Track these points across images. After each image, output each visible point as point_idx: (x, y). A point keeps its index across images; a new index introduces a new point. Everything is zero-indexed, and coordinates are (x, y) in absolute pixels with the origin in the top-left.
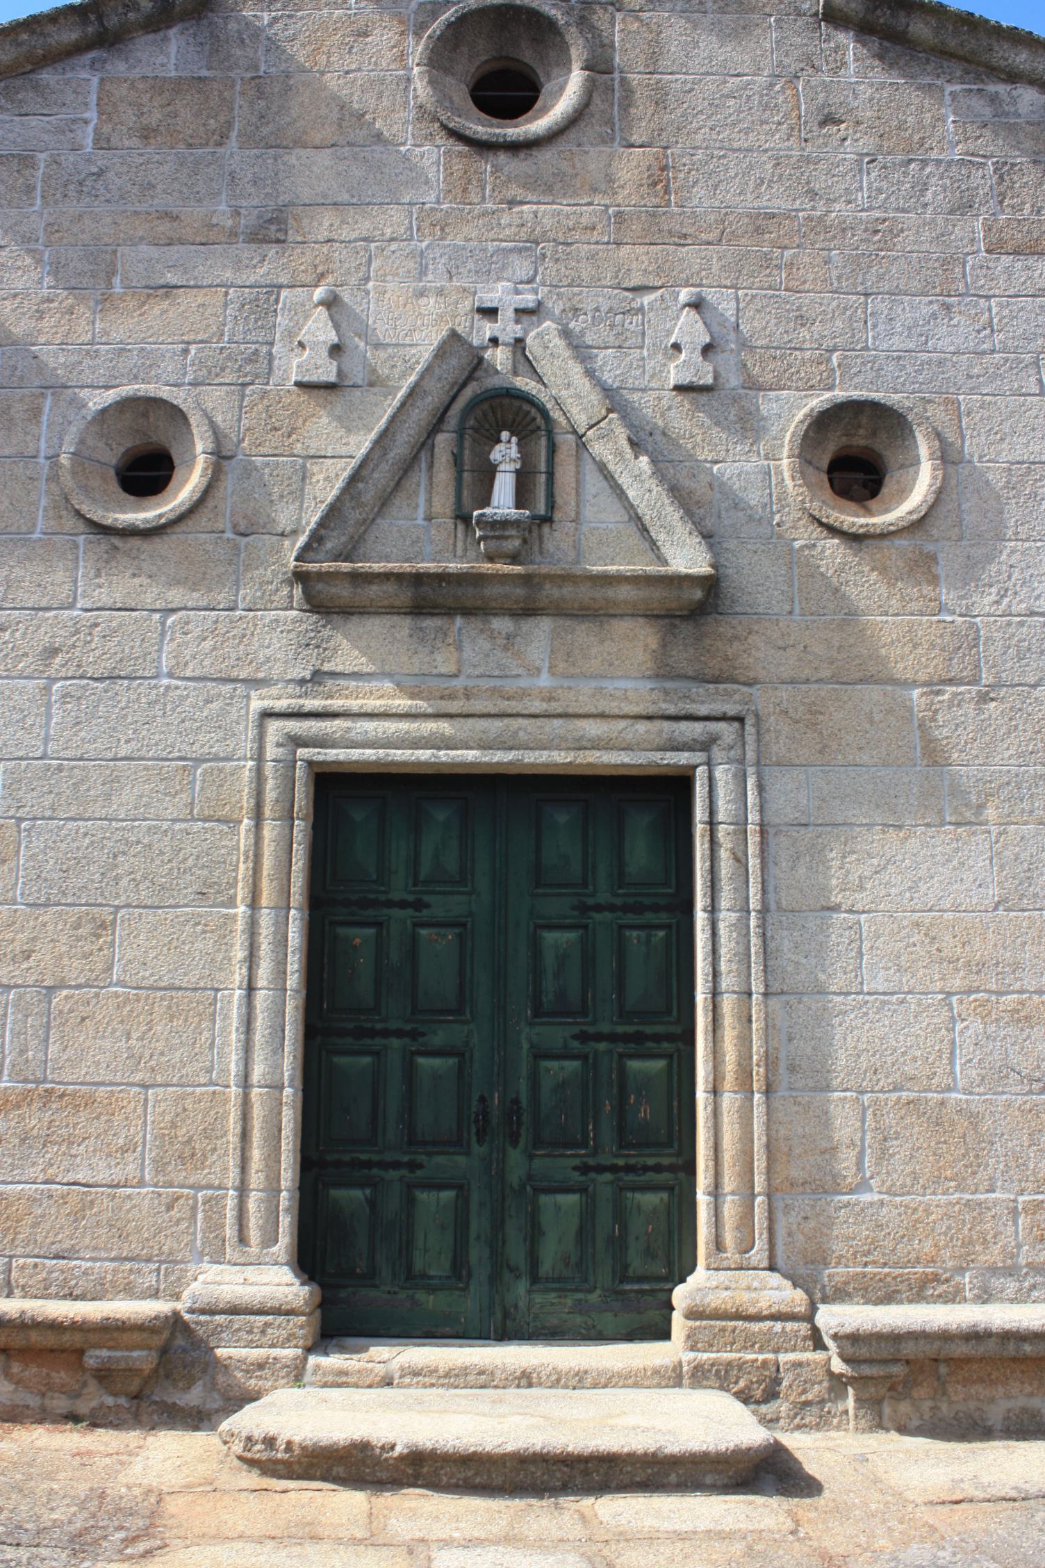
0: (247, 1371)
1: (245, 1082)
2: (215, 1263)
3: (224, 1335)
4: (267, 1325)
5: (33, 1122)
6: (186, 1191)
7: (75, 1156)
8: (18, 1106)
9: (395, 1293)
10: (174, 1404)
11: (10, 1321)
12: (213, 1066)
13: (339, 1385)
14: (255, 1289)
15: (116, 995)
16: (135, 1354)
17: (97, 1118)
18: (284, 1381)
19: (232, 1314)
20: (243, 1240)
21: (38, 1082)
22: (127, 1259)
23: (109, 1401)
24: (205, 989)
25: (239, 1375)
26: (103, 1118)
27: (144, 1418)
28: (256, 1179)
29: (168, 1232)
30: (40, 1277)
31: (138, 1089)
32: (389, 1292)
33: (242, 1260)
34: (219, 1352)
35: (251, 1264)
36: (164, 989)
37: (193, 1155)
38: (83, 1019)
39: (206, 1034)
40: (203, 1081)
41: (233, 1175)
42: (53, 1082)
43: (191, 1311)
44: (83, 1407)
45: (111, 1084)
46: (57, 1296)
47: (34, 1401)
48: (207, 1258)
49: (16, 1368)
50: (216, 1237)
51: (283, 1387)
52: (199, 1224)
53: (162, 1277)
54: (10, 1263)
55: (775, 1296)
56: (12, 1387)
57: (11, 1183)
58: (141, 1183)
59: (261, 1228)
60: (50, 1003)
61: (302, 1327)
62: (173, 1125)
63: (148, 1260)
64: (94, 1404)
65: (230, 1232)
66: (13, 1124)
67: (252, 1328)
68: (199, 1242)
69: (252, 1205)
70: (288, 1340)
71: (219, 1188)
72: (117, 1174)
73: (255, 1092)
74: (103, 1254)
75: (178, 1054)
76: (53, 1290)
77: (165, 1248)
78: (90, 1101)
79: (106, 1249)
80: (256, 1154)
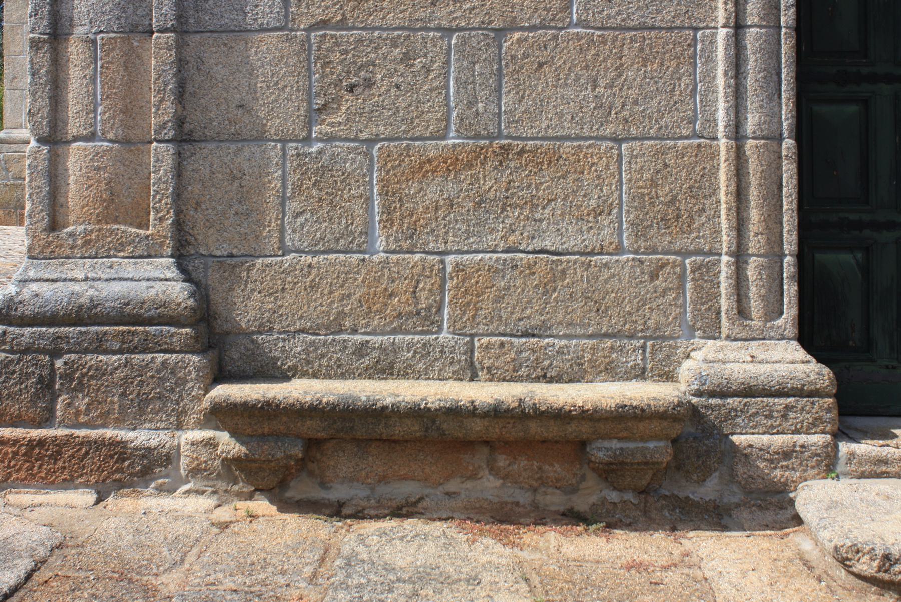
0: (771, 461)
1: (737, 133)
2: (709, 338)
3: (739, 420)
4: (788, 408)
5: (489, 184)
6: (672, 258)
7: (541, 221)
8: (469, 165)
9: (894, 368)
10: (687, 498)
11: (508, 410)
12: (695, 116)
13: (879, 476)
14: (768, 368)
15: (578, 37)
16: (651, 445)
17: (564, 177)
18: (816, 471)
19: (746, 396)
20: (742, 312)
21: (491, 137)
22: (606, 335)
23: (614, 496)
24: (682, 28)
25: (762, 465)
26: (571, 177)
27: (654, 514)
28: (755, 243)
29: (654, 305)
30: (508, 357)
31: (610, 144)
32: (887, 367)
33: (743, 335)
34: (735, 438)
35: (754, 339)
36: (634, 28)
37: (678, 217)
38: (540, 65)
39: (685, 80)
40: (685, 132)
41: (726, 239)
42: (507, 137)
43: (699, 393)
44: (582, 504)
45: (578, 138)
46: (529, 379)
47: (524, 498)
48: (698, 333)
49: (502, 461)
50: (709, 309)
51: (814, 478)
52: (688, 295)
53: (647, 355)
54: (472, 342)
55: (783, 369)
56: (499, 483)
57: (467, 252)
58: (619, 250)
59: (763, 298)
60: (500, 47)
61: (829, 410)
62: (653, 183)
63: (631, 336)
64: (593, 499)
65: (725, 303)
66: (464, 186)
67: (771, 411)
68: (689, 316)
69: (751, 273)
70: (814, 425)
71: (710, 253)
72: (590, 240)
73: (750, 143)
74: (579, 331)
75: (654, 103)
76: (523, 371)
77: (650, 323)
78: (554, 158)
79: (582, 325)
80: (754, 215)
